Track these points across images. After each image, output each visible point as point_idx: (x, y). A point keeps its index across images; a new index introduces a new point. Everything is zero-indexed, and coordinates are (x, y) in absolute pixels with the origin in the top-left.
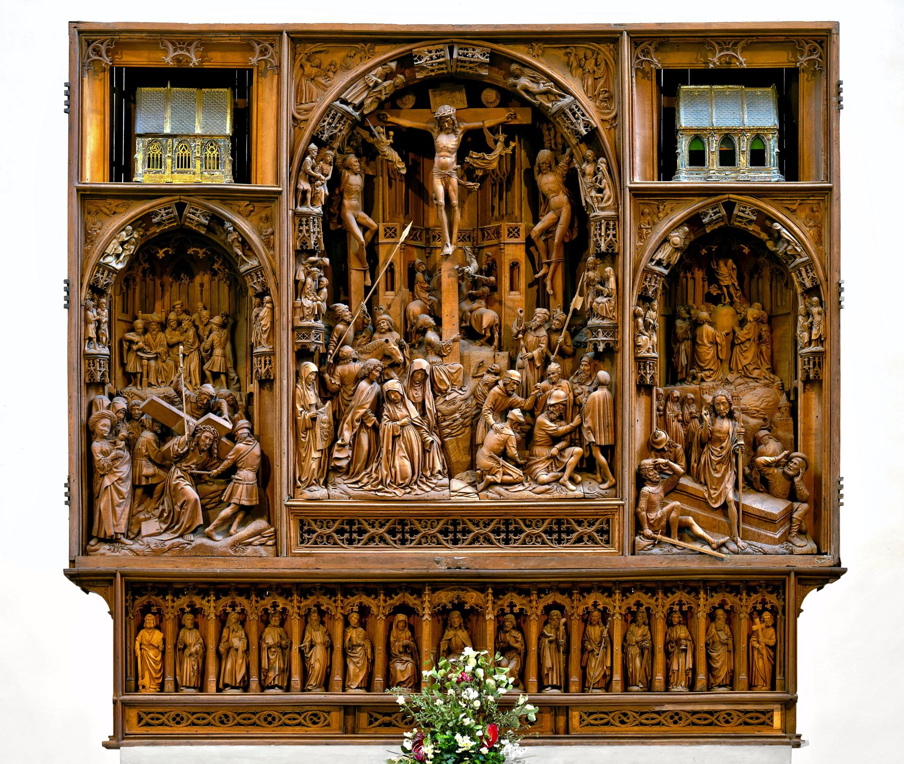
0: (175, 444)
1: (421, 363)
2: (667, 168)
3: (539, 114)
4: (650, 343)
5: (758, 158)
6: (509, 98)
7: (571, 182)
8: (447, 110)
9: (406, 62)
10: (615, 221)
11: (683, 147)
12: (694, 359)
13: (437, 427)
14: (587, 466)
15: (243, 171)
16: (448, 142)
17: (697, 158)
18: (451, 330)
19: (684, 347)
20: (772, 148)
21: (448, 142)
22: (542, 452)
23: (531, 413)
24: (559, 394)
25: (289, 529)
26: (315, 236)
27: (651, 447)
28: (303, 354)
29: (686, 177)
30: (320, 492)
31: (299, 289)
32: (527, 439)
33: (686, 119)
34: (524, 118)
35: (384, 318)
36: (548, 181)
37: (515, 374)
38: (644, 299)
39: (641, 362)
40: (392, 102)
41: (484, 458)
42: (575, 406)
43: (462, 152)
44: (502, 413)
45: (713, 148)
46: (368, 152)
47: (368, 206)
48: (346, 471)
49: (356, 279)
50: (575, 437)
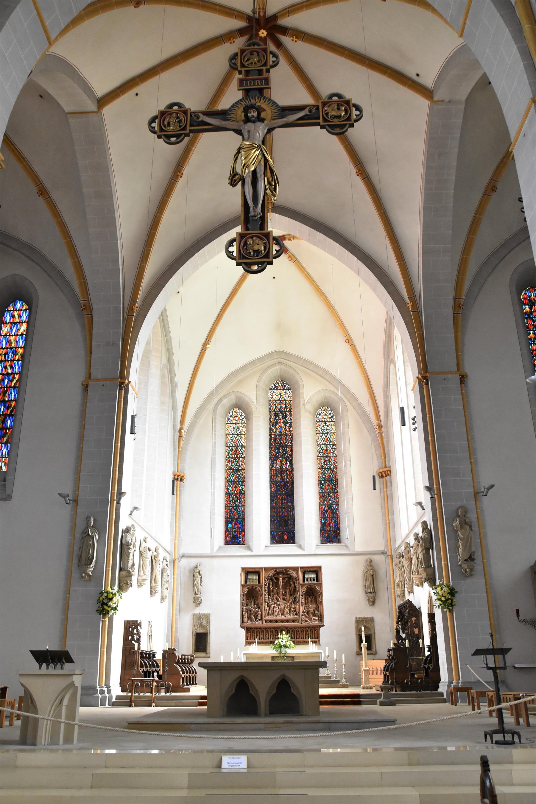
0: (252, 612)
1: (278, 603)
2: (304, 581)
3: (290, 576)
4: (303, 600)
5: (314, 580)
6: (287, 574)
7: (294, 583)
8: (281, 576)
9: (276, 571)
10: (299, 587)
11: (306, 579)
12: (308, 602)
13: (280, 610)
14: (296, 614)
15: (259, 582)
16: (281, 579)
17: (307, 580)
18: (282, 599)
19: (307, 601)
20: (315, 579)
21: (281, 579)
22: (291, 612)
23: (290, 608)
24: (293, 606)
25: (264, 622)
26: (267, 589)
27: (303, 612)
28: (265, 602)
29: (306, 582)
30: (267, 617)
31: (265, 595)
32: (290, 612)
33: (306, 576)
34: (289, 576)
35: (274, 598)
36: (292, 583)
37: (288, 604)
38: (302, 595)
39: (302, 602)
40: (274, 575)
41: (285, 614)
42: (295, 608)
43: (282, 580)
44: (287, 608)
45: (309, 579)
46: (272, 580)
47: (272, 586)
48: (271, 615)
49: (271, 594)
50: (295, 611)
